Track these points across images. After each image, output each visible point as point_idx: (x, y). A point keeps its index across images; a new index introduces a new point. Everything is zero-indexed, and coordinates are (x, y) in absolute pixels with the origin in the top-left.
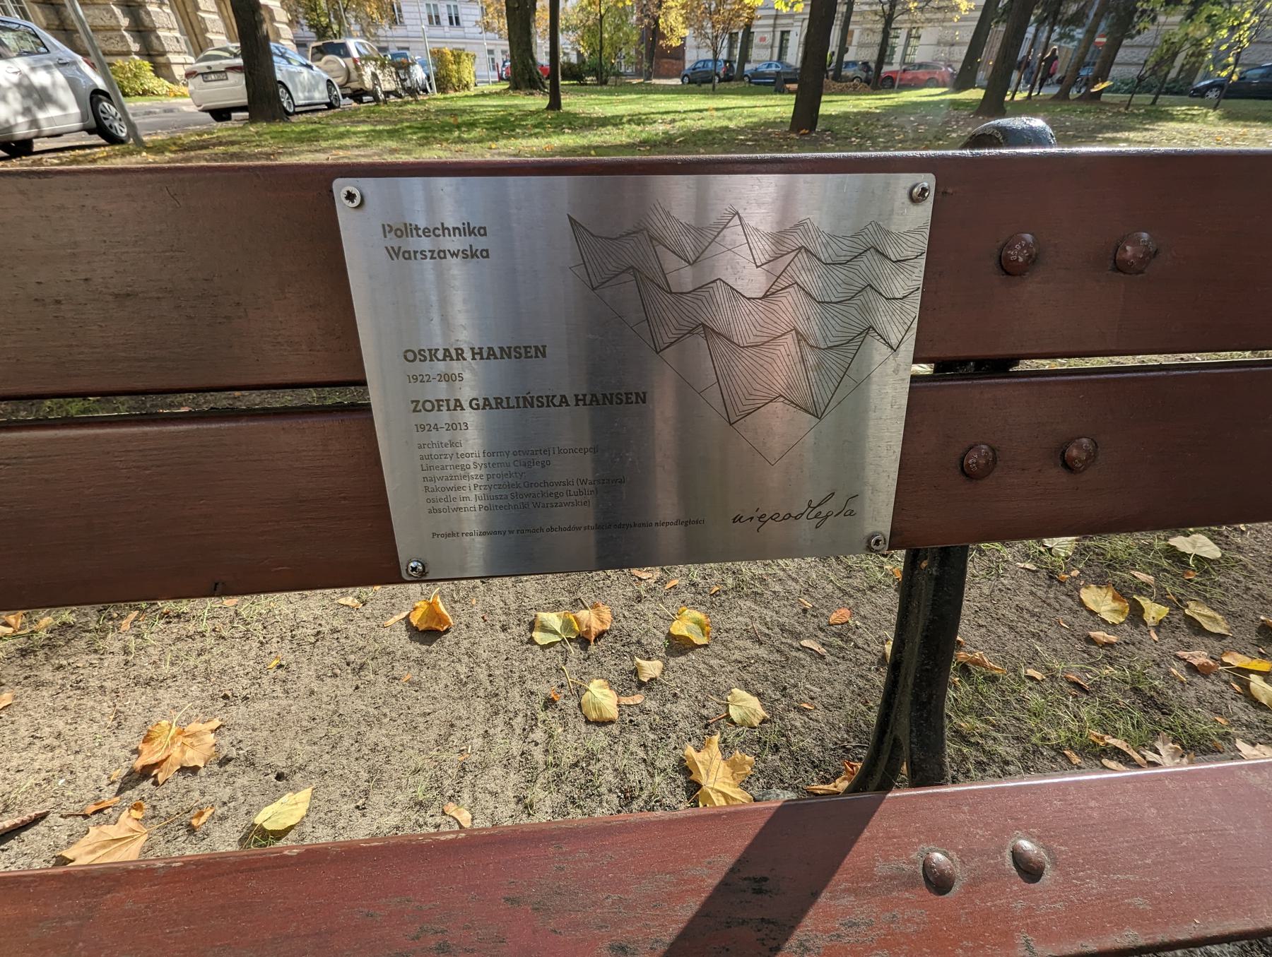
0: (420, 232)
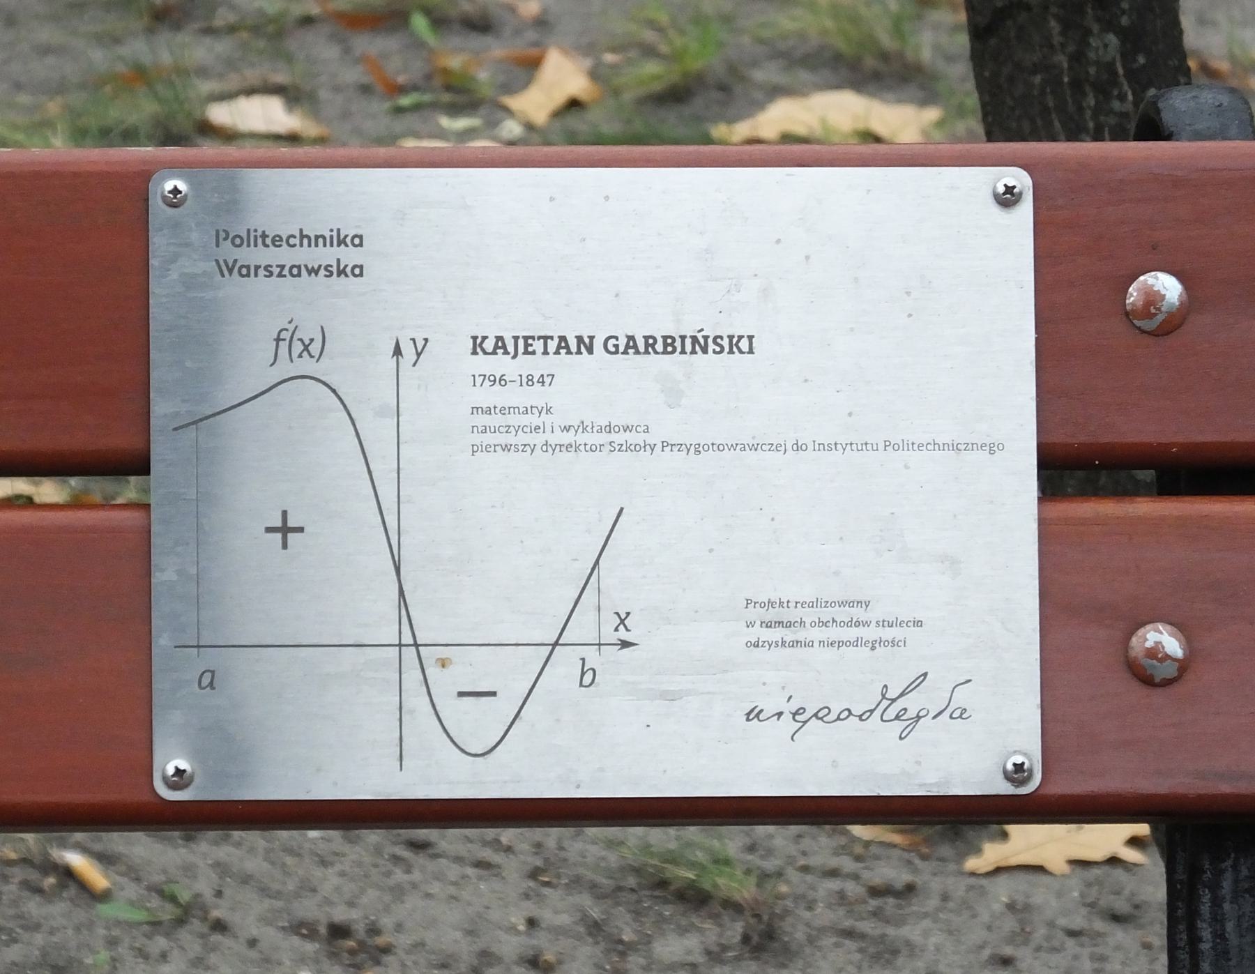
0: (268, 241)
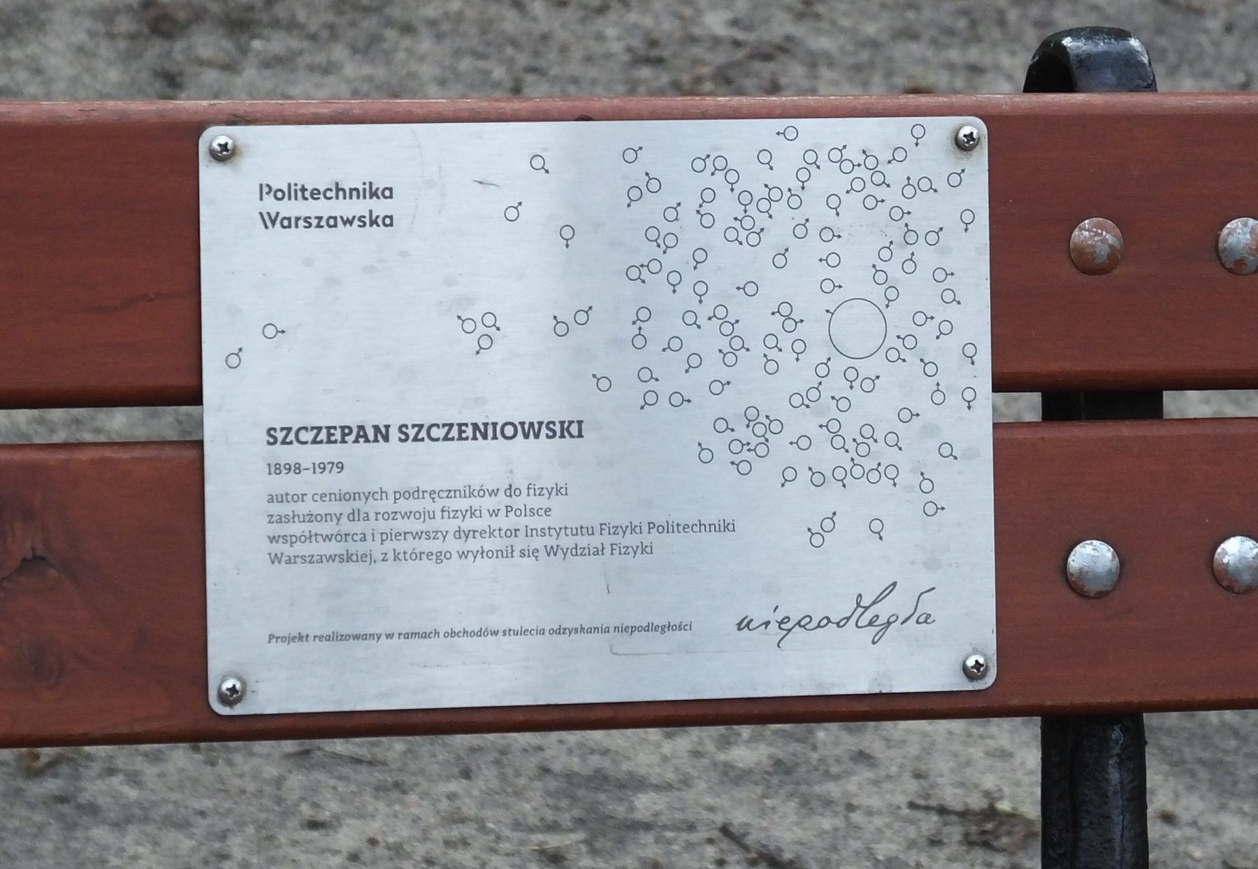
0: (307, 194)
